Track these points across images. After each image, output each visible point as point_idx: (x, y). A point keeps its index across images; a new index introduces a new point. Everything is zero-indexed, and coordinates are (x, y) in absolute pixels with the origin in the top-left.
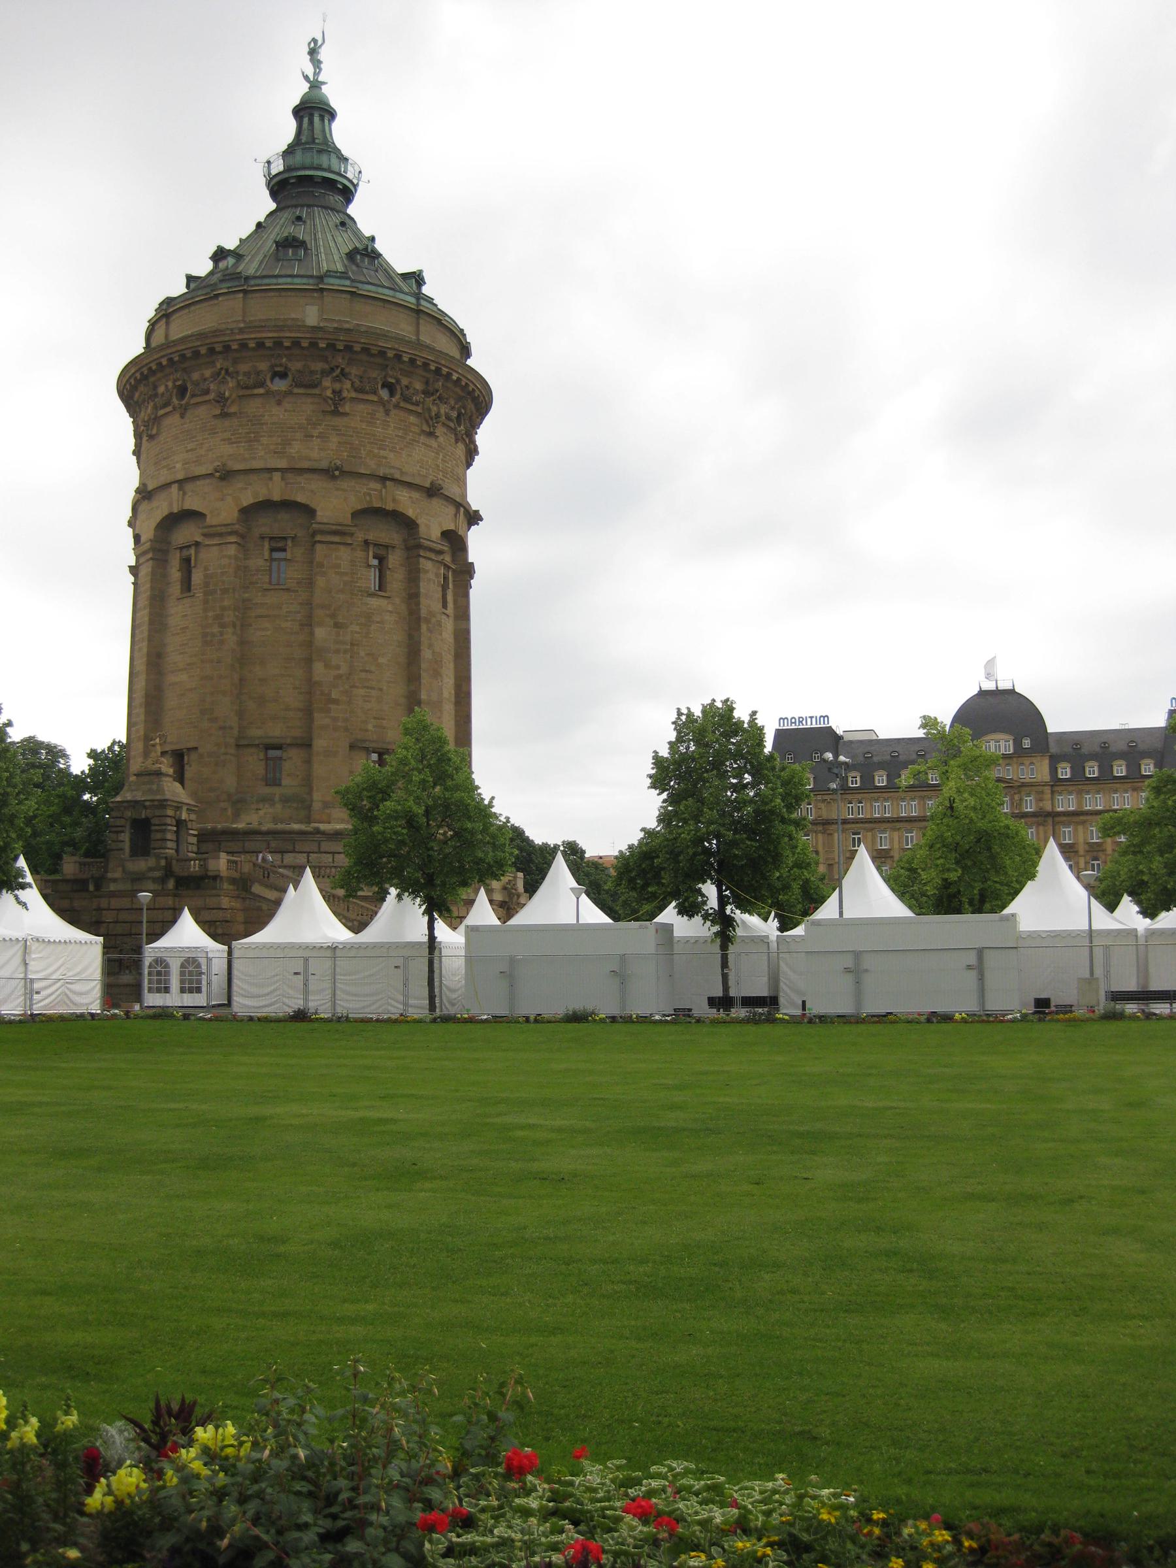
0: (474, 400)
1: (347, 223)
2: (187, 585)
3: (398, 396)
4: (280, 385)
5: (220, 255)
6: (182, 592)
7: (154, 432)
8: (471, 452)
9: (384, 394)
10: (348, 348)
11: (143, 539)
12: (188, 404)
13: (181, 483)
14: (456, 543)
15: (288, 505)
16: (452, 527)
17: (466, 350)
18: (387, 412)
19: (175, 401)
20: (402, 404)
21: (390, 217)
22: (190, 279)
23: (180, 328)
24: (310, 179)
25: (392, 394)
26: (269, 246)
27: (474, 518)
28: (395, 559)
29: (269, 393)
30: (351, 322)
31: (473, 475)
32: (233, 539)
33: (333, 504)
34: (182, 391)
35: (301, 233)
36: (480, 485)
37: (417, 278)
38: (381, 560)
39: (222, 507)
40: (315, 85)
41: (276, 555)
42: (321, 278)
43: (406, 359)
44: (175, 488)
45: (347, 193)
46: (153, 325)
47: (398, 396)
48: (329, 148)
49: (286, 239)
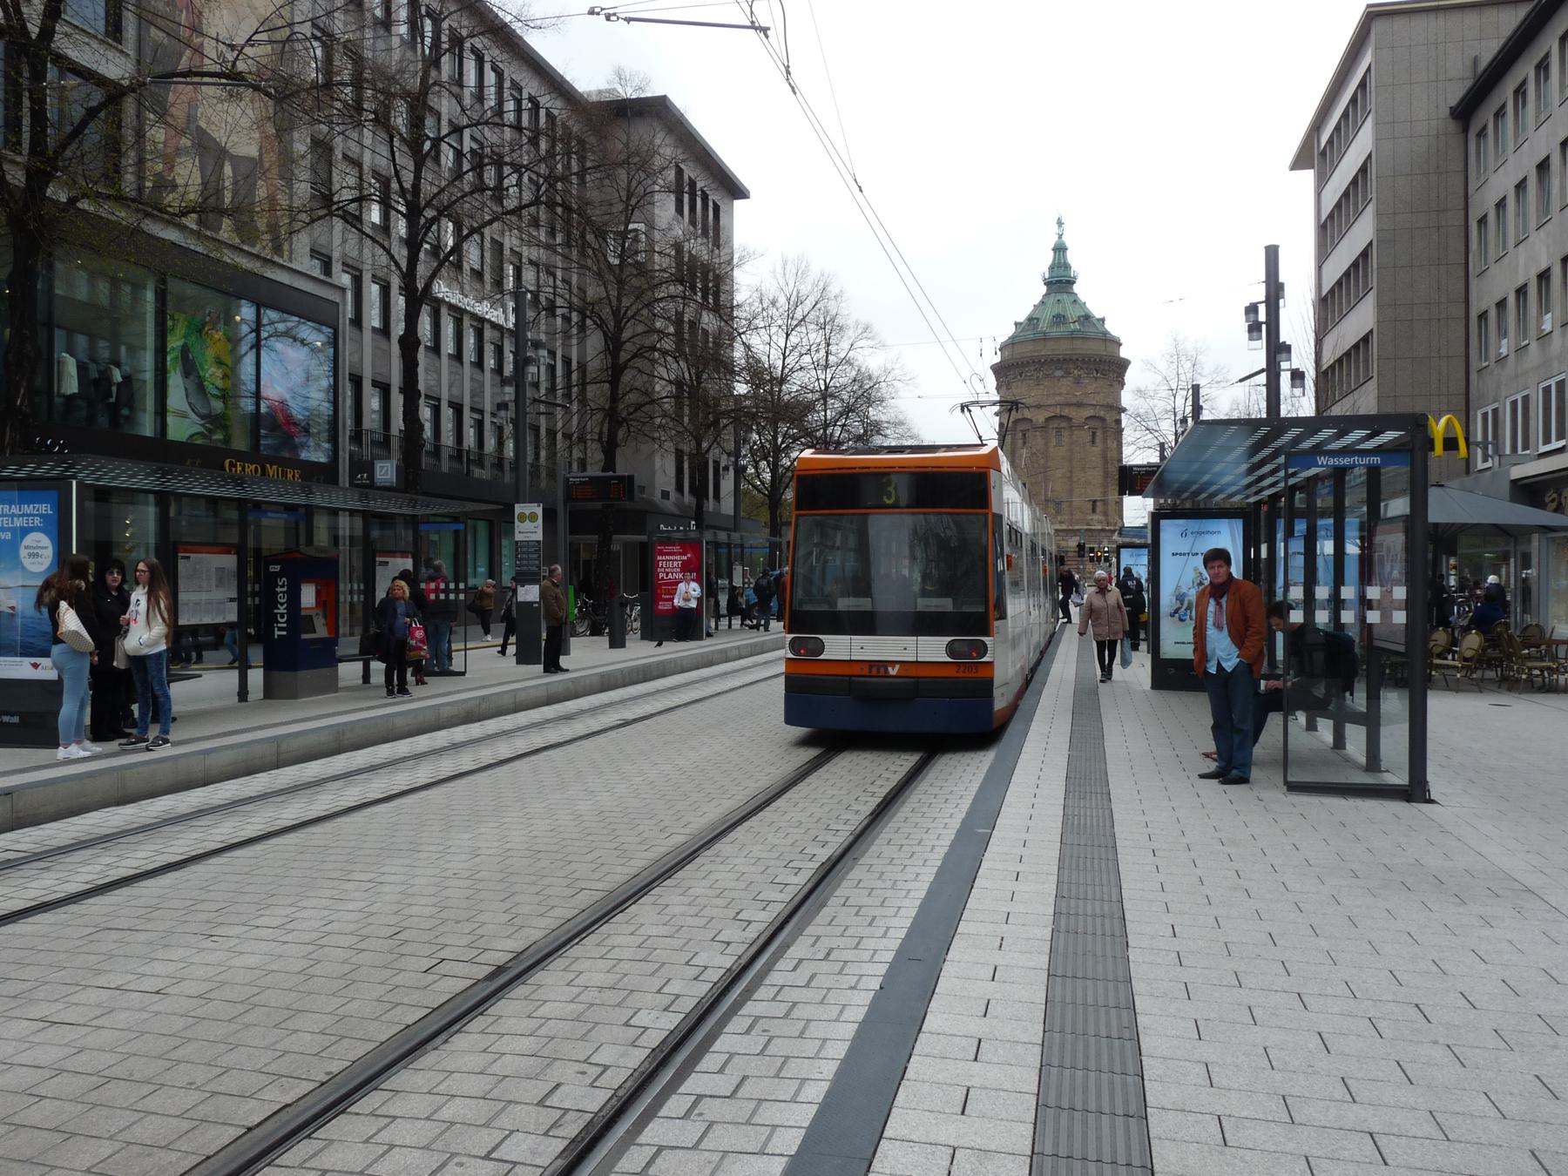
1: (1076, 301)
8: (1122, 384)
14: (1119, 422)
21: (1092, 294)
24: (1060, 281)
28: (1099, 433)
40: (1060, 236)
48: (1067, 267)
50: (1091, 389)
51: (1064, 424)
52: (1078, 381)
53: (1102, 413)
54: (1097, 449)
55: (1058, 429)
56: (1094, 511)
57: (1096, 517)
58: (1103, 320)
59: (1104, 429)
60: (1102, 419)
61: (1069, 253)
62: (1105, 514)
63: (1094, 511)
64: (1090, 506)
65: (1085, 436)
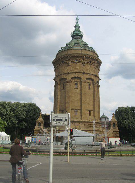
0: (99, 63)
4: (76, 61)
5: (67, 45)
8: (99, 71)
10: (86, 57)
14: (98, 82)
17: (98, 57)
18: (90, 65)
22: (62, 48)
23: (59, 55)
26: (73, 43)
27: (100, 80)
28: (91, 85)
30: (86, 53)
33: (84, 77)
35: (77, 42)
37: (92, 48)
38: (89, 85)
42: (82, 47)
45: (82, 37)
46: (58, 54)
50: (89, 68)
51: (79, 81)
52: (83, 64)
54: (91, 90)
55: (76, 83)
56: (90, 115)
57: (90, 117)
59: (93, 83)
60: (92, 80)
62: (94, 116)
63: (90, 115)
64: (88, 112)
65: (87, 85)
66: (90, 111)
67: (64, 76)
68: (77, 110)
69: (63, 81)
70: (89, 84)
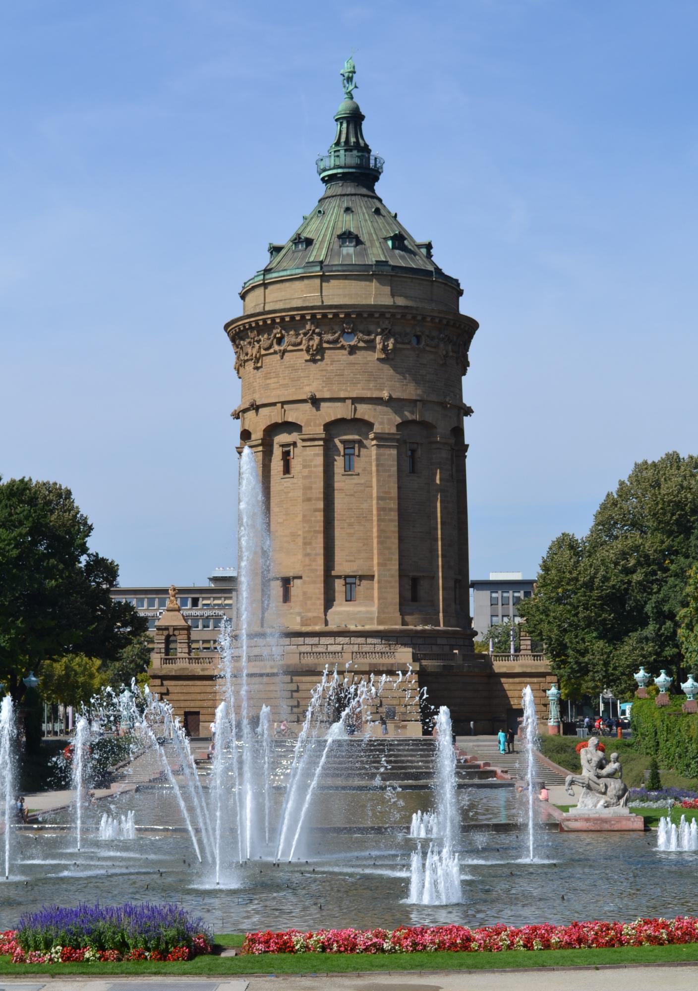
2: (287, 470)
3: (423, 343)
6: (284, 474)
7: (259, 365)
8: (464, 365)
9: (414, 341)
11: (253, 437)
12: (285, 351)
13: (283, 403)
14: (458, 432)
15: (355, 421)
16: (456, 425)
19: (276, 347)
20: (428, 348)
25: (418, 342)
27: (468, 411)
29: (343, 347)
31: (466, 381)
32: (321, 443)
34: (280, 341)
36: (472, 387)
38: (413, 451)
39: (313, 421)
41: (348, 451)
43: (429, 319)
44: (279, 405)
47: (423, 343)
49: (344, 233)
53: (429, 417)
58: (429, 246)
61: (364, 125)
66: (415, 581)
67: (293, 415)
68: (355, 577)
69: (282, 438)
70: (413, 451)
